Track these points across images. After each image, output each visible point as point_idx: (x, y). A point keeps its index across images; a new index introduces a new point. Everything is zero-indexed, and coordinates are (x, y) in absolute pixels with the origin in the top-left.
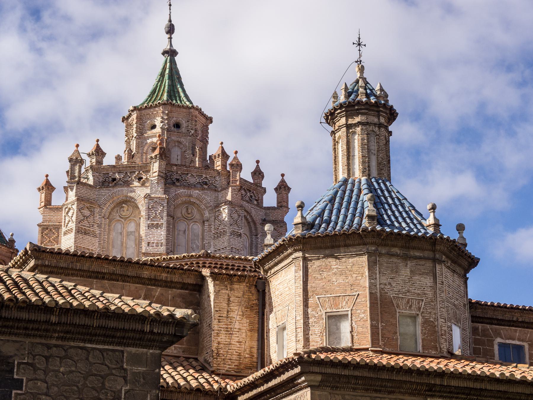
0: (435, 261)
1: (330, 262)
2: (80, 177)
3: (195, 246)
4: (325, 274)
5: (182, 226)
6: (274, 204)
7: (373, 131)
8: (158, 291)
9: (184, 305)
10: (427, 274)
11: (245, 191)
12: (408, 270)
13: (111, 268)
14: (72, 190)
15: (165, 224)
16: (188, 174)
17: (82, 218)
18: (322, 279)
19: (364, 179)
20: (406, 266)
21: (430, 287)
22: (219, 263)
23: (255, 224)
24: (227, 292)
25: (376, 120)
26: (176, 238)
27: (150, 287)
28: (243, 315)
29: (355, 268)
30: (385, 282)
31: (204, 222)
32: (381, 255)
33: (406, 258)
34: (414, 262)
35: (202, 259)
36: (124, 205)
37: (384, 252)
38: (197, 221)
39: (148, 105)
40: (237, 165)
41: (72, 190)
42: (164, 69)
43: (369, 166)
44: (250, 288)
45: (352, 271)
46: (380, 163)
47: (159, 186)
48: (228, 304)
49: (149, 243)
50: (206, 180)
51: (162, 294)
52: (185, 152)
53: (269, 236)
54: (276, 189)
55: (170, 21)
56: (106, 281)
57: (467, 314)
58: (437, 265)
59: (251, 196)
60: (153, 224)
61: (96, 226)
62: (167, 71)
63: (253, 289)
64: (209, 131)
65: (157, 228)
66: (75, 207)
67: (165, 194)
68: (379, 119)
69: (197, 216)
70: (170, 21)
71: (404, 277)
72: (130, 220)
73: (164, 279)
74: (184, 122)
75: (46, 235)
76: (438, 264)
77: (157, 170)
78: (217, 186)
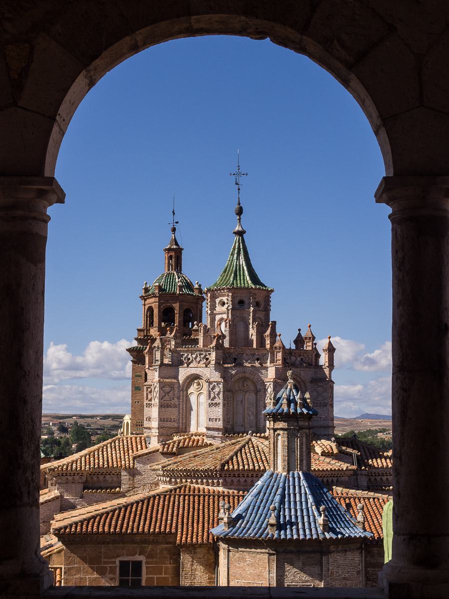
2: (162, 360)
3: (250, 413)
4: (242, 564)
5: (240, 397)
9: (169, 556)
11: (296, 357)
12: (301, 562)
14: (156, 371)
15: (221, 403)
16: (243, 354)
17: (164, 394)
18: (239, 568)
19: (284, 474)
20: (299, 560)
23: (304, 383)
26: (235, 407)
27: (143, 545)
29: (261, 563)
37: (281, 551)
39: (217, 288)
40: (280, 347)
41: (156, 371)
43: (288, 463)
44: (208, 551)
45: (258, 565)
49: (210, 419)
55: (239, 204)
56: (111, 545)
57: (361, 579)
58: (324, 557)
59: (302, 359)
60: (212, 403)
62: (236, 252)
63: (211, 552)
65: (215, 407)
66: (158, 385)
67: (221, 378)
69: (252, 388)
70: (239, 204)
74: (246, 299)
75: (149, 392)
76: (325, 555)
77: (214, 359)
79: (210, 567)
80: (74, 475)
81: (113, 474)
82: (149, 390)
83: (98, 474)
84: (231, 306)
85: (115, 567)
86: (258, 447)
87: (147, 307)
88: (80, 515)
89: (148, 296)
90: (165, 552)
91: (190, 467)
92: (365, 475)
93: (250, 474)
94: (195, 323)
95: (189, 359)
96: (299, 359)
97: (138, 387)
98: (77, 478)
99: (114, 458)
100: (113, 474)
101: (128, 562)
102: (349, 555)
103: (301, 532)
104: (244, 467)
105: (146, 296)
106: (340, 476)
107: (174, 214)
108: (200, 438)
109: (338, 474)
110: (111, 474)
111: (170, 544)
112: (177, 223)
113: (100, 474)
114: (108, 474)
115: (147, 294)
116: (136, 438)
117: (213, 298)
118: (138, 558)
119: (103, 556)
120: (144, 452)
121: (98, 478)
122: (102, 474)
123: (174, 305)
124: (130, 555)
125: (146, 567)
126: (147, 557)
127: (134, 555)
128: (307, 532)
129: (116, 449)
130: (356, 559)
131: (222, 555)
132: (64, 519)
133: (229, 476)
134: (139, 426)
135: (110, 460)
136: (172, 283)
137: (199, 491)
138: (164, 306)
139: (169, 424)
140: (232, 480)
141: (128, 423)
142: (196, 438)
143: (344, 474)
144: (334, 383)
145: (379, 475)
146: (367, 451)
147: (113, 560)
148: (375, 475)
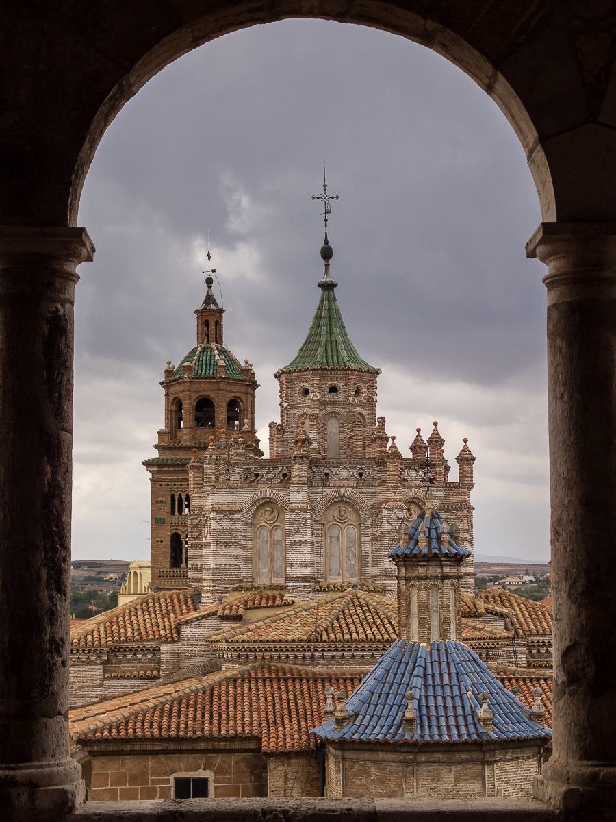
0: (484, 763)
1: (368, 767)
3: (351, 555)
6: (457, 480)
7: (435, 584)
8: (218, 759)
9: (249, 770)
10: (475, 778)
11: (416, 470)
12: (453, 776)
13: (165, 746)
18: (360, 786)
20: (450, 772)
21: (478, 793)
22: (333, 646)
24: (284, 768)
25: (439, 570)
27: (210, 755)
28: (302, 793)
30: (424, 794)
31: (360, 524)
32: (419, 764)
33: (449, 763)
34: (460, 767)
35: (313, 644)
36: (267, 509)
38: (353, 523)
42: (320, 308)
46: (443, 623)
47: (301, 493)
48: (285, 782)
49: (291, 564)
50: (361, 471)
51: (224, 761)
52: (343, 424)
53: (329, 701)
54: (457, 459)
55: (326, 242)
60: (295, 541)
61: (238, 536)
63: (313, 761)
64: (376, 385)
68: (442, 569)
70: (326, 242)
71: (447, 785)
72: (276, 526)
73: (222, 748)
74: (341, 386)
78: (375, 477)
79: (312, 786)
80: (89, 653)
81: (148, 650)
82: (196, 522)
83: (125, 651)
84: (318, 395)
85: (169, 789)
86: (367, 606)
87: (171, 398)
88: (107, 711)
89: (173, 381)
90: (243, 764)
91: (271, 635)
92: (524, 645)
93: (360, 646)
94: (246, 421)
95: (257, 475)
96: (421, 473)
97: (160, 519)
98: (93, 657)
99: (149, 625)
100: (148, 650)
101: (188, 780)
102: (523, 764)
103: (454, 731)
104: (351, 635)
105: (171, 382)
106: (487, 648)
107: (209, 258)
108: (276, 593)
109: (488, 644)
110: (145, 649)
111: (251, 752)
112: (214, 271)
113: (127, 650)
114: (139, 649)
115: (170, 381)
116: (178, 597)
117: (290, 383)
118: (202, 774)
119: (150, 772)
120: (194, 616)
121: (125, 655)
122: (130, 650)
123: (211, 394)
124: (191, 771)
125: (216, 787)
126: (216, 773)
127: (196, 769)
128: (463, 730)
129: (149, 612)
130: (532, 769)
131: (332, 766)
132: (83, 719)
133: (329, 650)
134: (163, 576)
135: (142, 629)
136: (210, 360)
137: (285, 673)
138: (197, 398)
139: (227, 574)
140: (333, 656)
141: (135, 573)
142: (270, 593)
143: (498, 644)
144: (473, 509)
145: (544, 645)
146: (524, 609)
147: (166, 778)
148: (539, 645)
